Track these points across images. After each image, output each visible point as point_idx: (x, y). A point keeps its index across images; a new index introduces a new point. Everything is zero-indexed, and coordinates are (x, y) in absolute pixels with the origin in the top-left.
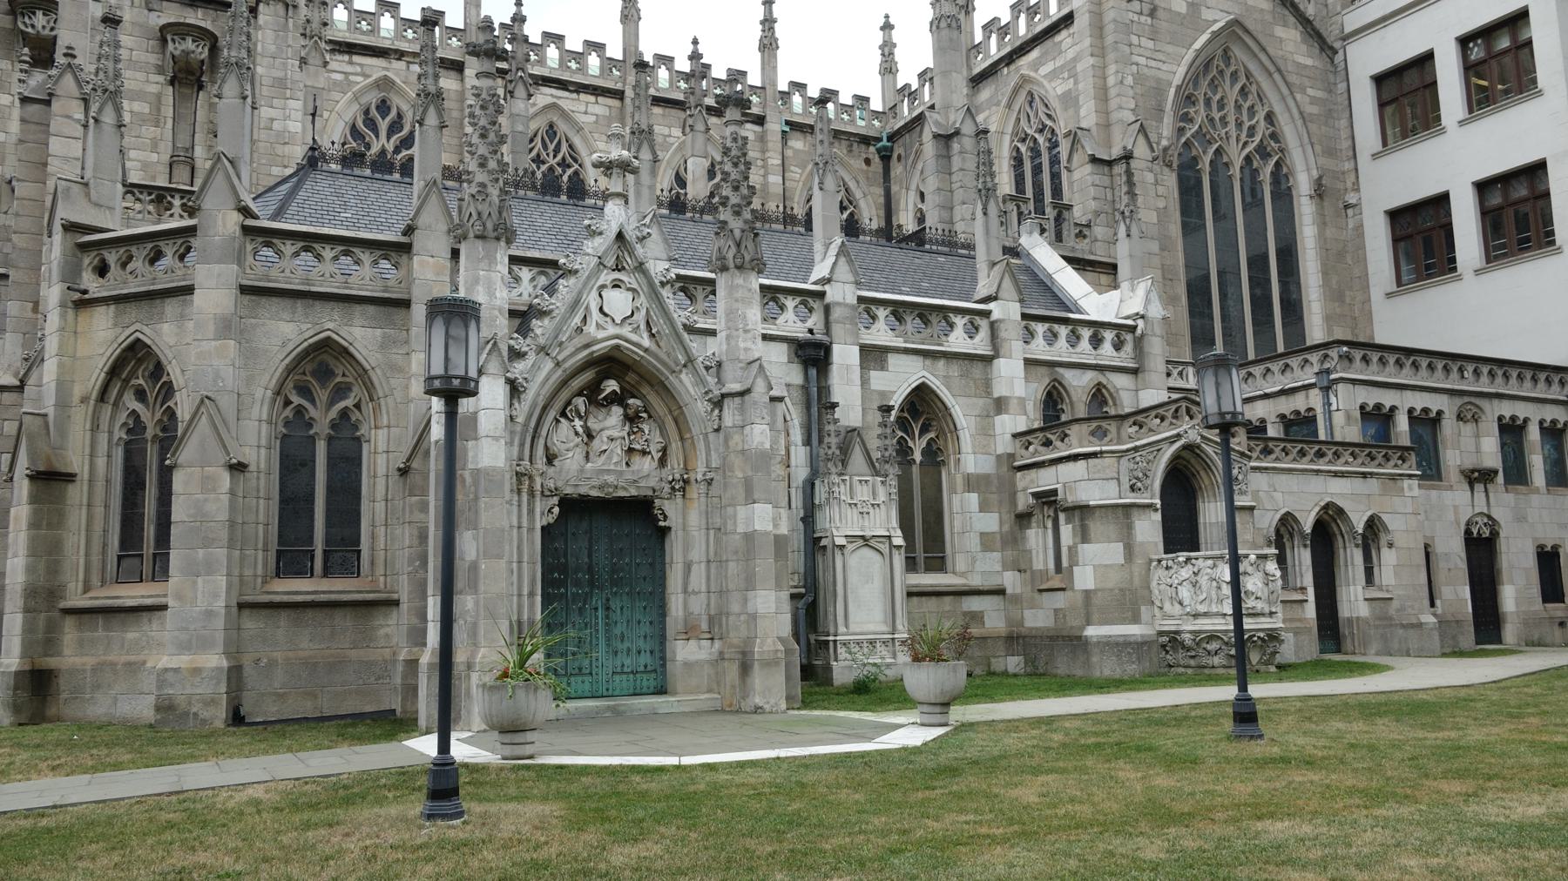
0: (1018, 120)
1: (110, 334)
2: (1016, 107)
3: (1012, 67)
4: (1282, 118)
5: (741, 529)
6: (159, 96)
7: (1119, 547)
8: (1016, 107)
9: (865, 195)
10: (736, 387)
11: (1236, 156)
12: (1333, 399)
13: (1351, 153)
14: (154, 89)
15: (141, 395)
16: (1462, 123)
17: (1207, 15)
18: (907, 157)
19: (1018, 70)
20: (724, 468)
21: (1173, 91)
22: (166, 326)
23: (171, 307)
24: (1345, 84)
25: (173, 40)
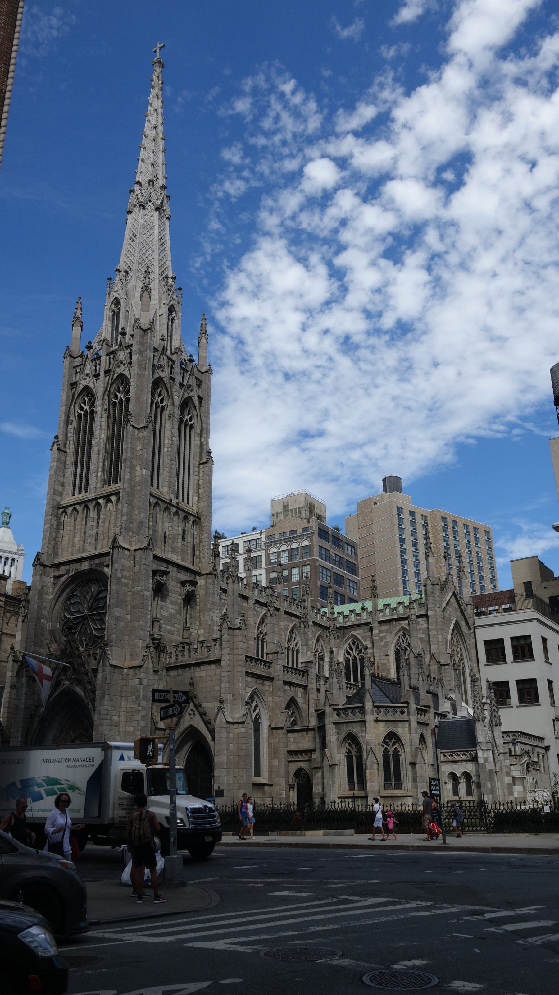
0: (398, 640)
1: (384, 729)
2: (398, 636)
3: (398, 623)
4: (463, 649)
5: (506, 782)
6: (180, 604)
7: (522, 787)
8: (398, 636)
9: (326, 648)
10: (502, 751)
11: (457, 660)
12: (517, 747)
13: (476, 661)
14: (179, 601)
15: (387, 743)
16: (512, 662)
17: (452, 618)
18: (344, 638)
19: (400, 624)
20: (501, 769)
21: (448, 642)
22: (399, 729)
23: (400, 724)
24: (474, 640)
25: (189, 586)
